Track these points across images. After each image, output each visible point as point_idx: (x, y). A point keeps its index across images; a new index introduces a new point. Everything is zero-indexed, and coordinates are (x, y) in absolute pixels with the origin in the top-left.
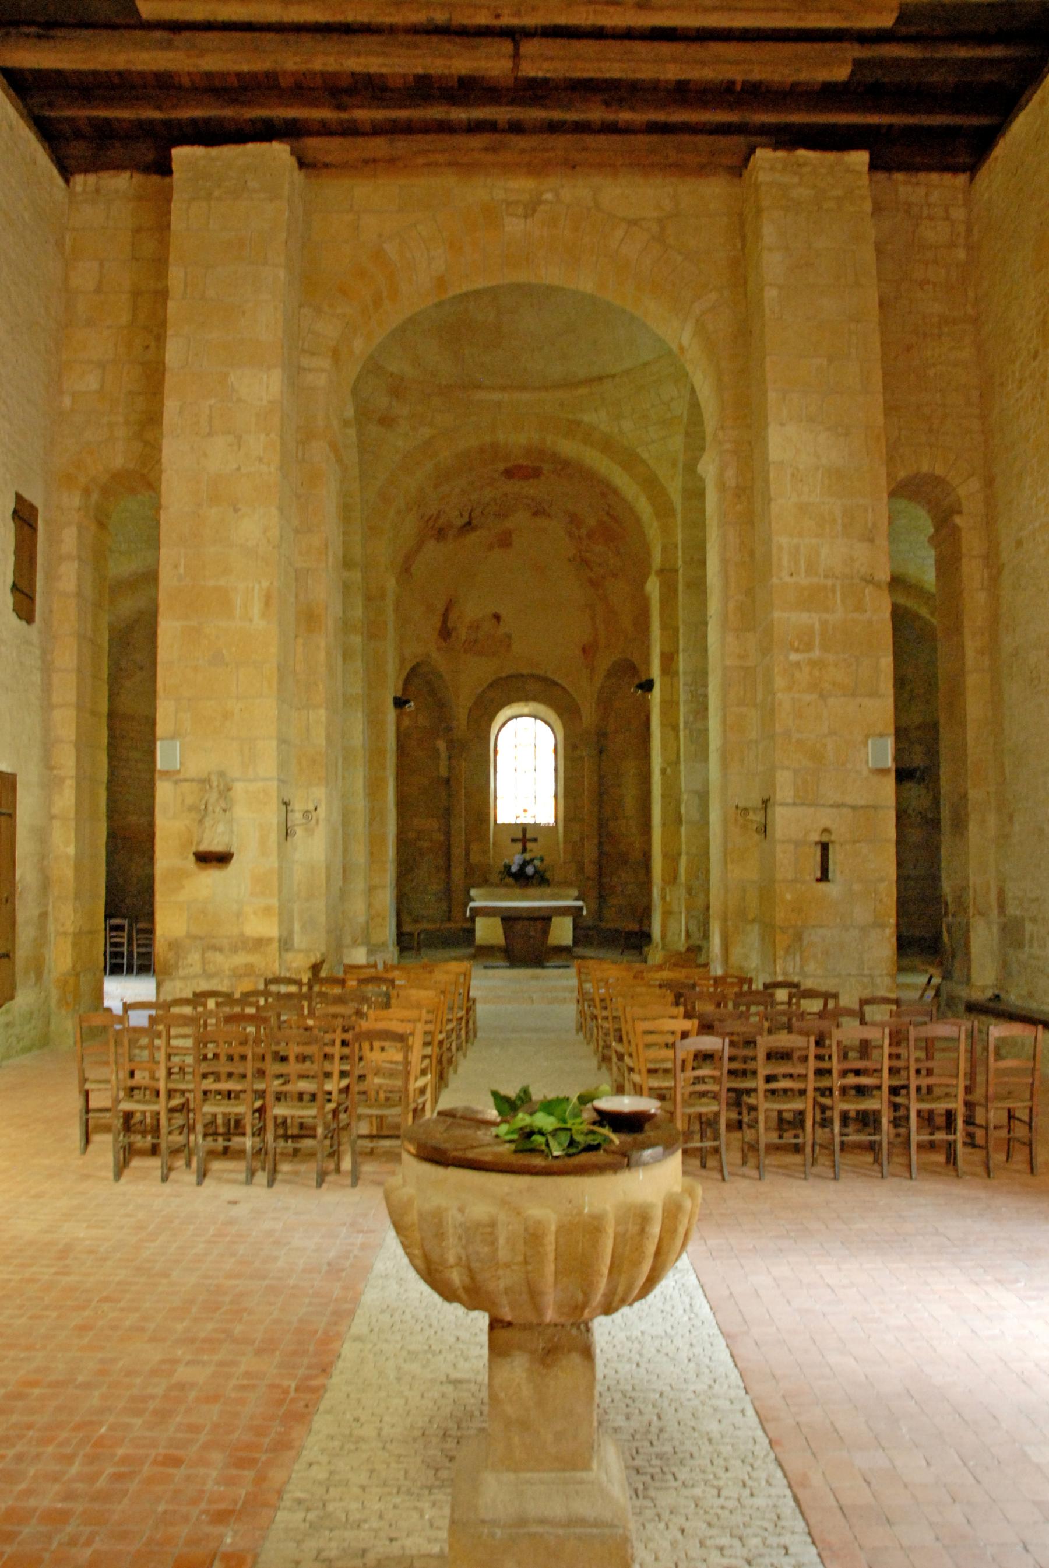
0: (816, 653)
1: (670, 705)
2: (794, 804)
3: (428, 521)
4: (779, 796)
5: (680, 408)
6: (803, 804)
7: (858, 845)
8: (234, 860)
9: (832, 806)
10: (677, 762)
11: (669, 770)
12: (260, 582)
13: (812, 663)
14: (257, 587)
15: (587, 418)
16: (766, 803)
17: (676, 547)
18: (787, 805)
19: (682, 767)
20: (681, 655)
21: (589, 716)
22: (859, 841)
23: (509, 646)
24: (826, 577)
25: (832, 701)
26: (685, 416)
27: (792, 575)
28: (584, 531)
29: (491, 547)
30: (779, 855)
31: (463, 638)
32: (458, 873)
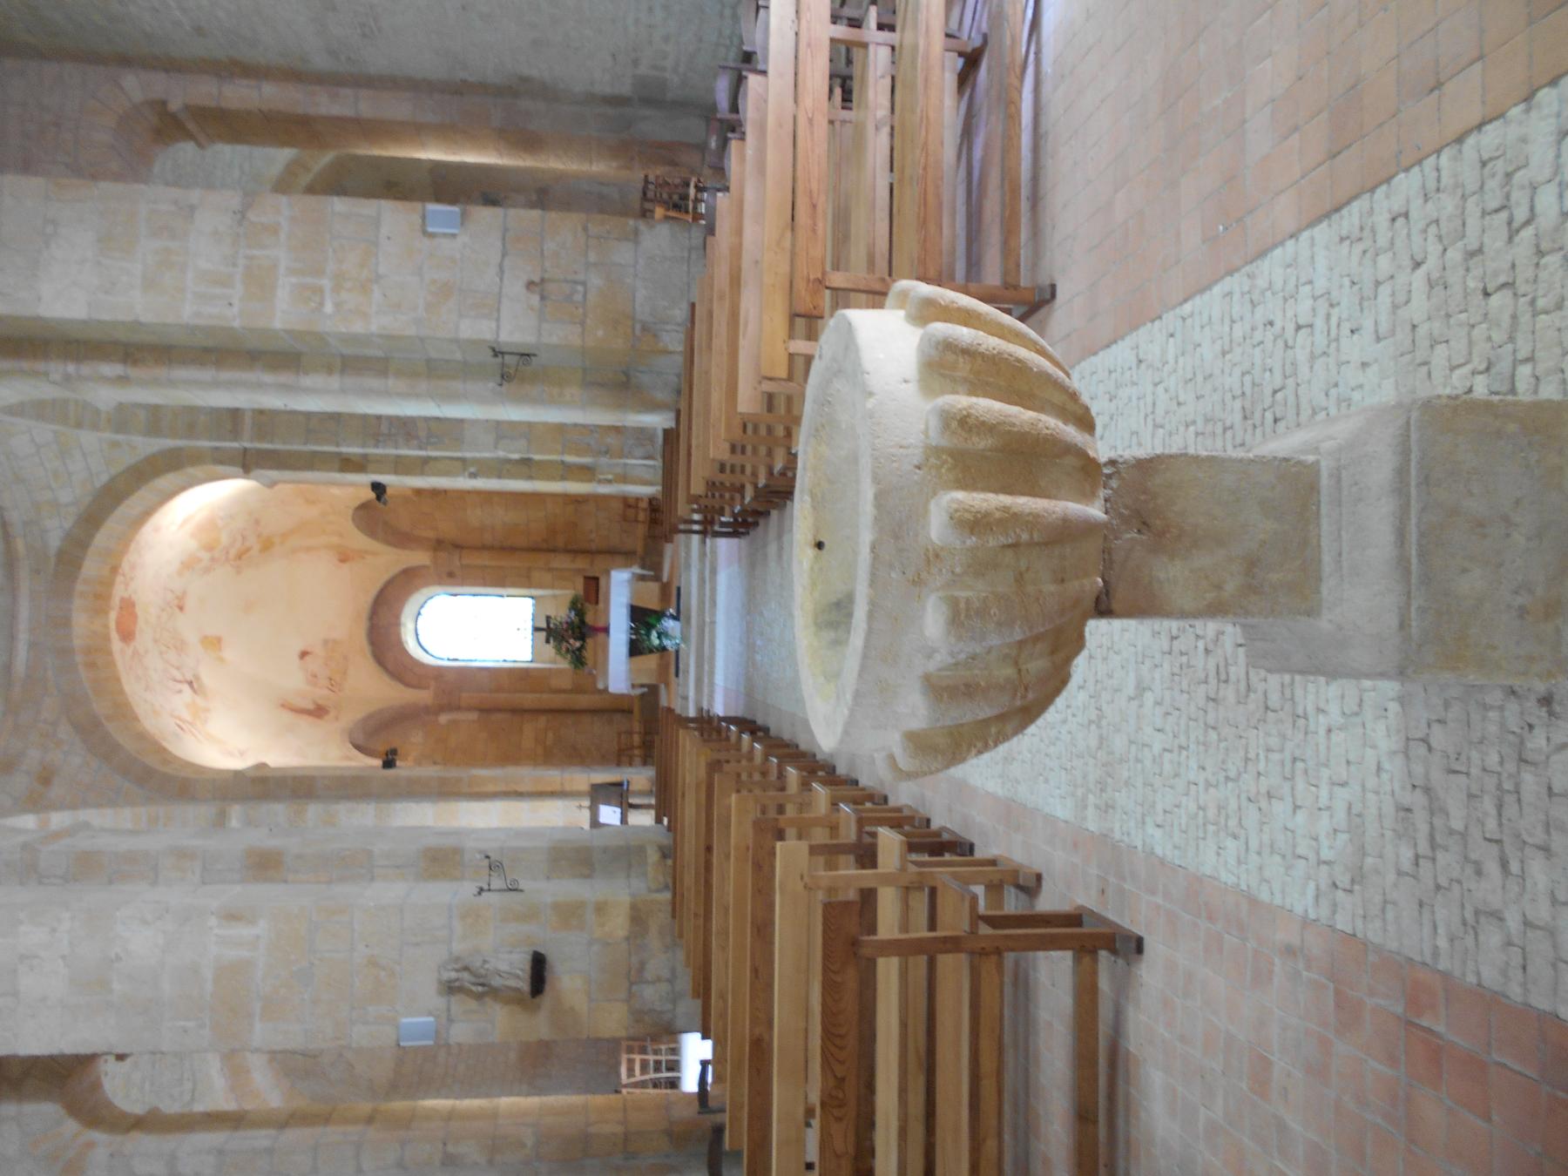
0: (326, 283)
1: (401, 466)
2: (498, 320)
4: (489, 336)
5: (45, 431)
6: (498, 310)
7: (546, 253)
8: (542, 951)
9: (501, 279)
10: (463, 460)
11: (472, 470)
12: (211, 928)
13: (337, 288)
14: (216, 931)
15: (54, 541)
16: (496, 353)
17: (217, 449)
18: (498, 327)
19: (468, 455)
20: (344, 450)
21: (420, 558)
22: (542, 251)
24: (234, 265)
25: (382, 270)
26: (53, 427)
27: (230, 304)
29: (221, 660)
30: (554, 340)
31: (326, 692)
32: (583, 701)
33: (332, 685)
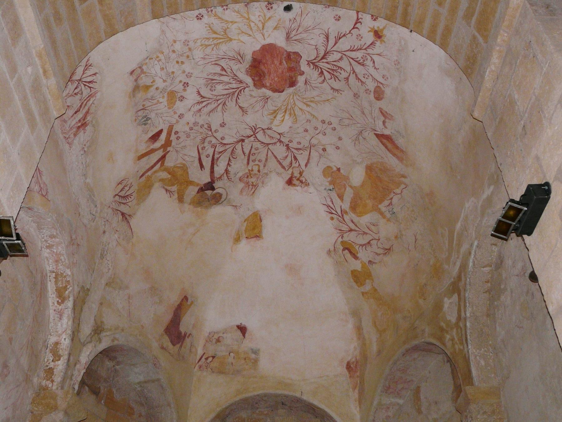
3: (155, 137)
23: (256, 361)
28: (349, 194)
29: (237, 240)
31: (200, 352)
33: (207, 359)
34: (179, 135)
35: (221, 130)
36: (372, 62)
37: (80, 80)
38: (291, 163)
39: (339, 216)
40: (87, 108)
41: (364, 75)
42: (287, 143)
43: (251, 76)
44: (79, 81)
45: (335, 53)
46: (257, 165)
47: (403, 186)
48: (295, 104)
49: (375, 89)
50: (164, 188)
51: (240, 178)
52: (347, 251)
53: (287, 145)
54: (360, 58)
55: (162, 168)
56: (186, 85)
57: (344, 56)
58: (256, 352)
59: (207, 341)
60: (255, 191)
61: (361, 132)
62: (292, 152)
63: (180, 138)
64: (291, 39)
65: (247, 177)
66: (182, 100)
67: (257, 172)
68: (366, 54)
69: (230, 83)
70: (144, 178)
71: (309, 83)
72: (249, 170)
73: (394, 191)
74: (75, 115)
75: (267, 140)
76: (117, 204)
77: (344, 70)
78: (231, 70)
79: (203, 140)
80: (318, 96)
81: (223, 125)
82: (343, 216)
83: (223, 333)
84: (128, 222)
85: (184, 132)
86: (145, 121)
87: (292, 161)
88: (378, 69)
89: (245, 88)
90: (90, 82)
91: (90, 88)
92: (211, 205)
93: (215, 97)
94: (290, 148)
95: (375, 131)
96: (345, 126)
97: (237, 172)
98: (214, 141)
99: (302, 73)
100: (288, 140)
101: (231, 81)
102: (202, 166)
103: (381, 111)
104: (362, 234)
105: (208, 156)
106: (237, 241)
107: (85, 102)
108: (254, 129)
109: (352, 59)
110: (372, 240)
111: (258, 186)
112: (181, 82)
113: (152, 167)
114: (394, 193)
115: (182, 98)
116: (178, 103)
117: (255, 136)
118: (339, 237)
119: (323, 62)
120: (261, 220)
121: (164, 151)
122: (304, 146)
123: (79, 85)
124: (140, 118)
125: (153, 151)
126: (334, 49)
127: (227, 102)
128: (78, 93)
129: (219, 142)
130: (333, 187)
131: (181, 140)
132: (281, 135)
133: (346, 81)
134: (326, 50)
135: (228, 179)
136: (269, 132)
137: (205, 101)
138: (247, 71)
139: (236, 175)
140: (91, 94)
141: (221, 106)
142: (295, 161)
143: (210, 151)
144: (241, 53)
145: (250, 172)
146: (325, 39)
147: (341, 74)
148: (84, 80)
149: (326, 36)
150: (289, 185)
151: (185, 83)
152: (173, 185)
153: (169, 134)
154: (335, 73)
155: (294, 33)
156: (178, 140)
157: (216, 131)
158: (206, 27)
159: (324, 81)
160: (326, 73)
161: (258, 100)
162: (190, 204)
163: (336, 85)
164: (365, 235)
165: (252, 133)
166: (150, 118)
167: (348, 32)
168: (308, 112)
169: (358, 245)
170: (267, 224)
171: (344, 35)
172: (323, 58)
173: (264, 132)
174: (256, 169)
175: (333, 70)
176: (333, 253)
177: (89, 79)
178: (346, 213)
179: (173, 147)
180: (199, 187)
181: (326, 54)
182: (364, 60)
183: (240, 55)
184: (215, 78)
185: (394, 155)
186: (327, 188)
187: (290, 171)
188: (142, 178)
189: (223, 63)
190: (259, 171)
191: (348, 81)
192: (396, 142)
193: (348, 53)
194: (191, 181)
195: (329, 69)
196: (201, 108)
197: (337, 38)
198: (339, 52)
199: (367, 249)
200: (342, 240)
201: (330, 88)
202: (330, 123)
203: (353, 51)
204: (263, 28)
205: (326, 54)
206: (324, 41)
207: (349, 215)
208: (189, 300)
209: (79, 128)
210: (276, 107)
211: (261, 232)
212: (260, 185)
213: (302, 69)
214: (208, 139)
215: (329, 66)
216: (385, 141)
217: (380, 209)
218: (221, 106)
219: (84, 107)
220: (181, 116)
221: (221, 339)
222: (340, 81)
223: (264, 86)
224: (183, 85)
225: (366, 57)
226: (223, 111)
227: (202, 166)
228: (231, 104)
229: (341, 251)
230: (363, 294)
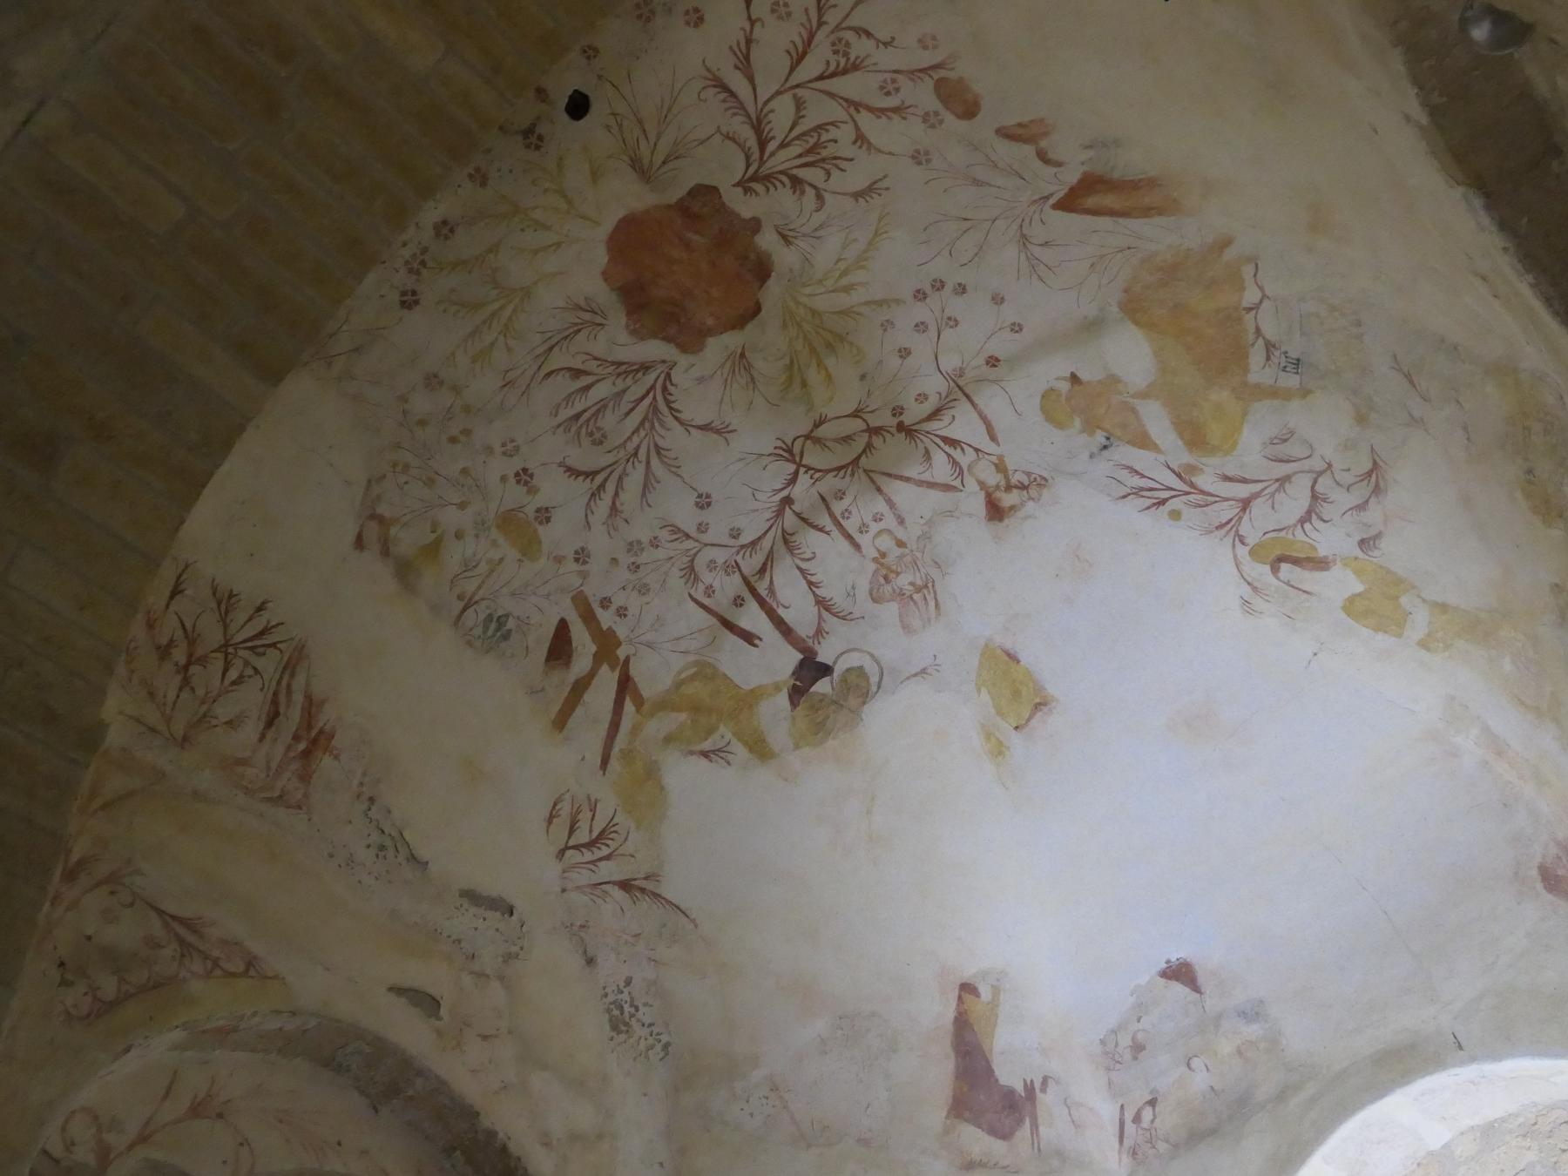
3: (560, 648)
28: (1156, 420)
29: (999, 751)
33: (1137, 1119)
34: (618, 601)
35: (707, 516)
36: (863, 36)
37: (226, 645)
38: (955, 463)
39: (1187, 493)
40: (298, 698)
41: (882, 88)
42: (895, 421)
43: (654, 335)
44: (224, 649)
45: (773, 105)
46: (880, 533)
47: (1248, 271)
48: (814, 312)
49: (939, 96)
50: (692, 753)
51: (871, 594)
52: (1285, 567)
53: (901, 427)
54: (833, 59)
55: (646, 707)
56: (524, 477)
57: (799, 92)
58: (1253, 1013)
59: (1108, 1069)
60: (936, 599)
61: (1023, 236)
62: (928, 432)
63: (626, 609)
64: (655, 168)
65: (886, 578)
66: (548, 520)
67: (898, 551)
68: (832, 32)
69: (624, 391)
70: (614, 764)
71: (791, 234)
72: (875, 560)
73: (1245, 304)
74: (270, 734)
75: (845, 455)
76: (584, 872)
77: (832, 124)
78: (596, 359)
79: (691, 573)
80: (844, 247)
81: (704, 502)
82: (1192, 485)
83: (1139, 1021)
84: (657, 896)
85: (624, 588)
86: (497, 630)
87: (949, 455)
88: (893, 38)
89: (668, 375)
90: (262, 633)
91: (274, 645)
92: (856, 713)
93: (622, 453)
94: (914, 428)
95: (1047, 198)
96: (976, 259)
97: (849, 588)
98: (721, 556)
99: (755, 225)
100: (889, 413)
101: (620, 385)
102: (749, 638)
103: (1005, 134)
104: (1277, 490)
105: (738, 602)
106: (1000, 753)
107: (284, 683)
108: (785, 454)
109: (821, 78)
110: (1315, 482)
111: (933, 581)
112: (504, 479)
113: (615, 726)
114: (1249, 310)
115: (544, 515)
116: (542, 531)
117: (804, 466)
118: (1234, 546)
119: (772, 154)
120: (1013, 658)
121: (613, 668)
122: (940, 394)
123: (230, 657)
124: (478, 631)
125: (580, 688)
126: (761, 101)
127: (661, 443)
128: (241, 677)
129: (734, 550)
130: (1105, 434)
131: (633, 611)
132: (864, 416)
133: (864, 148)
134: (748, 116)
135: (844, 618)
136: (822, 432)
137: (606, 480)
138: (633, 333)
139: (854, 595)
140: (290, 658)
141: (655, 462)
142: (959, 449)
143: (733, 584)
144: (583, 304)
145: (882, 565)
146: (723, 96)
147: (836, 141)
148: (239, 638)
149: (715, 86)
150: (1001, 519)
151: (517, 474)
152: (710, 731)
153: (589, 617)
154: (824, 153)
155: (645, 150)
156: (625, 616)
157: (702, 528)
158: (445, 311)
159: (819, 197)
160: (802, 173)
161: (725, 376)
162: (797, 747)
163: (856, 177)
164: (1287, 485)
165: (792, 468)
166: (507, 616)
167: (747, 27)
168: (867, 303)
169: (1295, 526)
170: (1037, 656)
171: (749, 41)
172: (762, 145)
173: (818, 441)
174: (885, 543)
175: (809, 151)
176: (1258, 603)
177: (250, 631)
178: (1192, 469)
179: (630, 642)
180: (785, 691)
181: (758, 126)
182: (846, 54)
183: (581, 309)
184: (579, 407)
185: (1147, 212)
186: (1095, 450)
187: (971, 484)
188: (609, 768)
189: (558, 360)
190: (900, 544)
191: (869, 143)
192: (1116, 175)
193: (799, 76)
194: (752, 691)
195: (800, 156)
196: (614, 503)
197: (741, 66)
198: (778, 93)
199: (1326, 519)
200: (1248, 548)
201: (851, 199)
202: (938, 284)
203: (804, 54)
204: (569, 202)
205: (758, 126)
206: (724, 101)
207: (1205, 468)
208: (985, 992)
209: (306, 754)
210: (782, 358)
211: (1039, 689)
212: (935, 573)
213: (746, 213)
214: (700, 563)
215: (795, 150)
216: (1091, 201)
217: (1257, 386)
218: (655, 462)
219: (289, 700)
220: (581, 556)
221: (1140, 1036)
222: (852, 160)
223: (703, 334)
224: (518, 482)
225: (840, 40)
226: (674, 469)
227: (749, 638)
228: (674, 438)
229: (1271, 579)
230: (1424, 644)
